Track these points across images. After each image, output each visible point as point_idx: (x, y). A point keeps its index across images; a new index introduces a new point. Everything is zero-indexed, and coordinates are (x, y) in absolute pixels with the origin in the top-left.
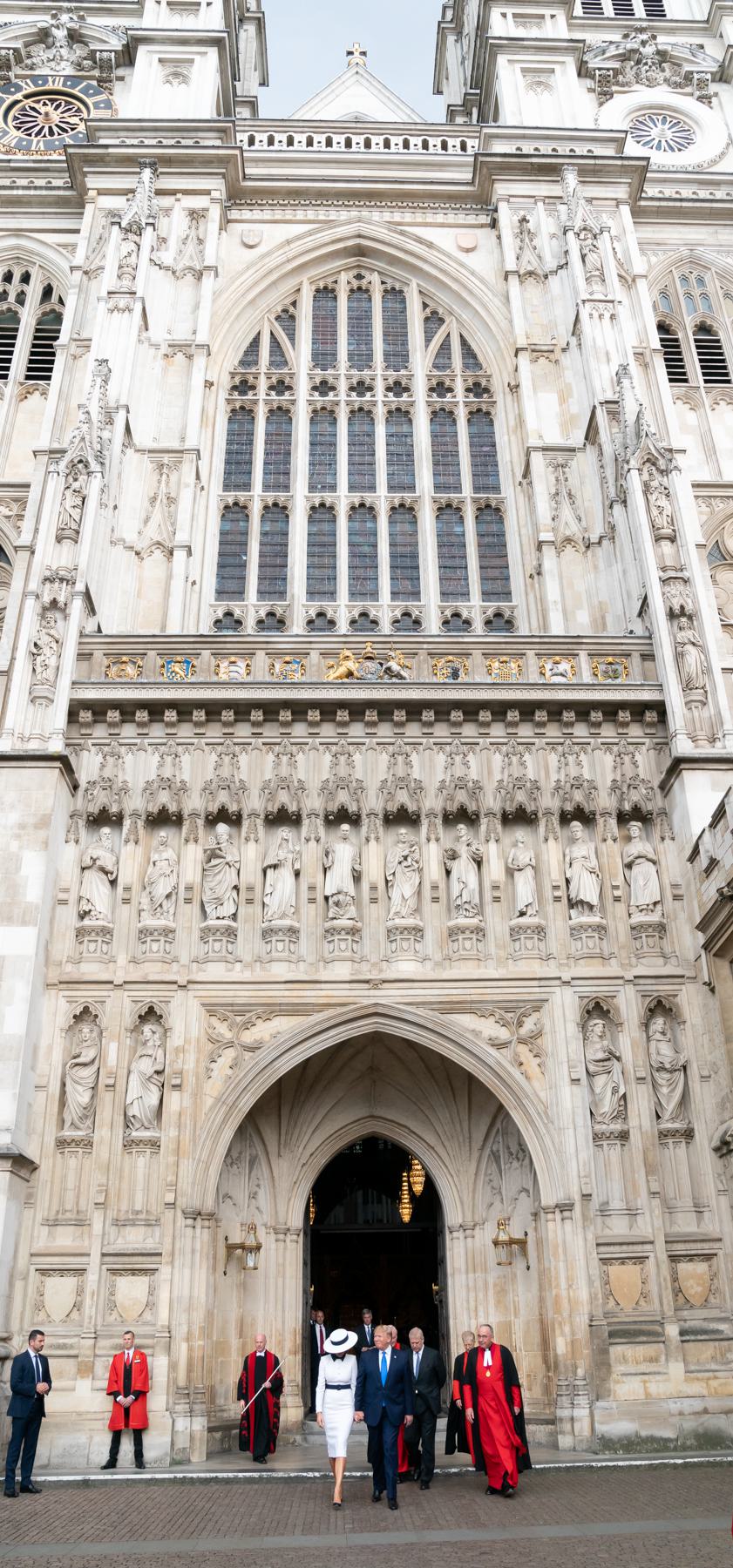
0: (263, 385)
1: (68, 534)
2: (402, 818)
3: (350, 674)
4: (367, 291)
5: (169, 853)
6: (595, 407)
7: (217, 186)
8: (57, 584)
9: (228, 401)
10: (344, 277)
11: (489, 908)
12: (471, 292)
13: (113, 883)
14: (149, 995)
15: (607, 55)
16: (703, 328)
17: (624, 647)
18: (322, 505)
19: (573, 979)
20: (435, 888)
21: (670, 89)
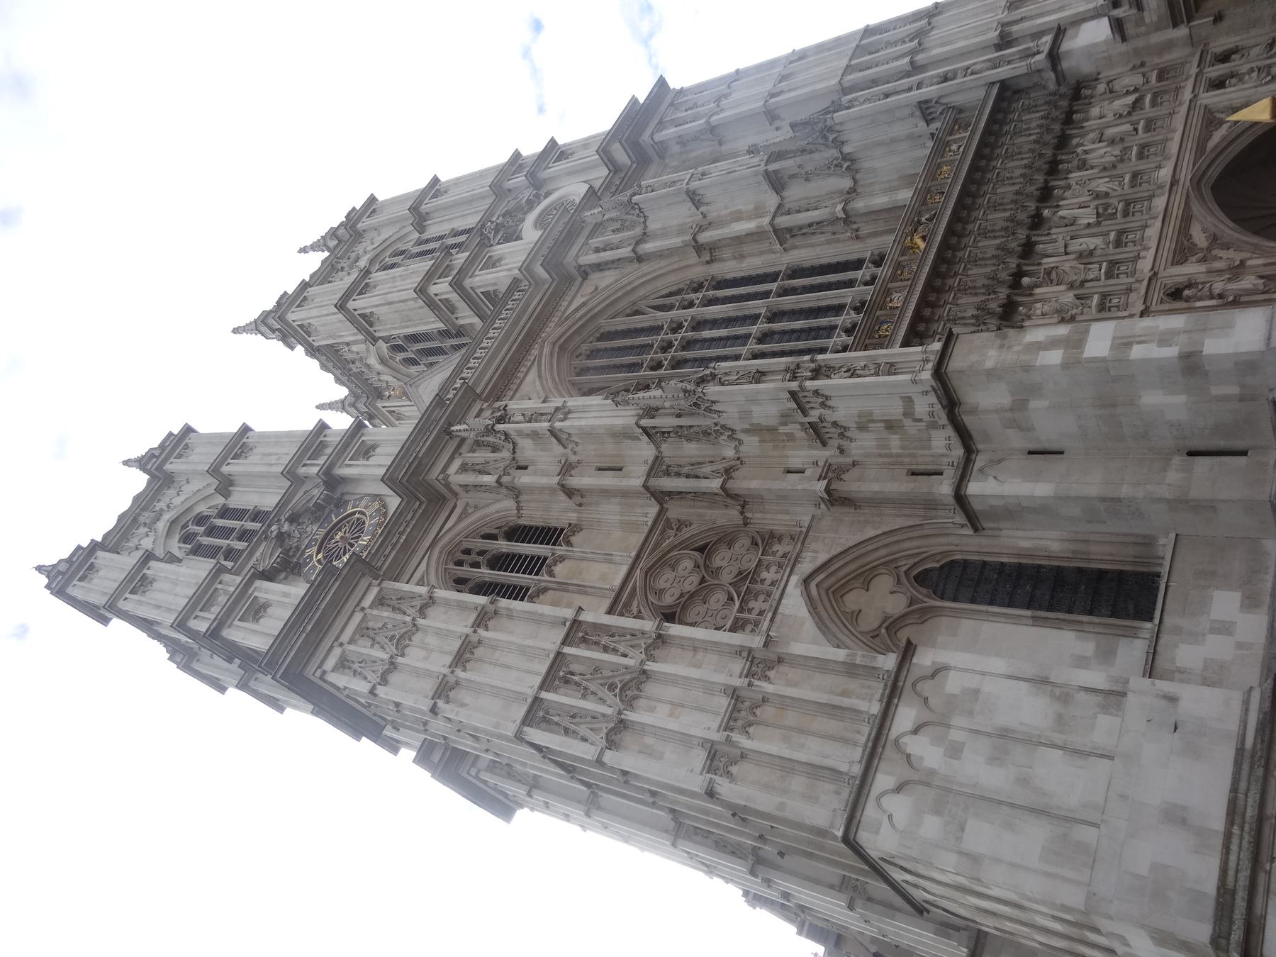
1: (759, 376)
3: (924, 238)
5: (1039, 305)
6: (766, 171)
10: (576, 362)
11: (1126, 145)
12: (629, 283)
14: (1156, 295)
17: (950, 122)
19: (1193, 91)
20: (1105, 169)
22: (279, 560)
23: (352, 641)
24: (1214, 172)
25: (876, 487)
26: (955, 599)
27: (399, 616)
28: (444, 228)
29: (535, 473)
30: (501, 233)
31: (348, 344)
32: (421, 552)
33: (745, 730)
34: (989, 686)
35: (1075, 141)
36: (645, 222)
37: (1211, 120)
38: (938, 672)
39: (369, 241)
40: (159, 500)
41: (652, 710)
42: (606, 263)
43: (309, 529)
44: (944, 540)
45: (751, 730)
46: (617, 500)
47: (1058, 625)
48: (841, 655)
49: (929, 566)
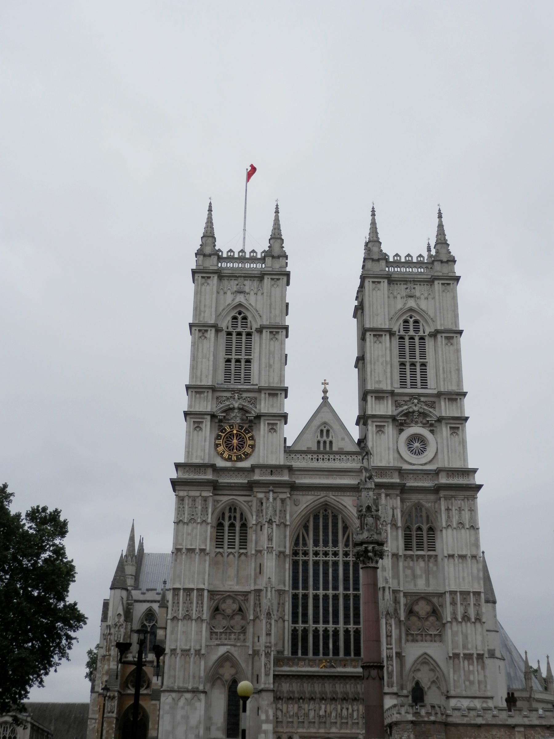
0: (301, 552)
1: (268, 634)
2: (333, 699)
3: (324, 666)
4: (328, 516)
5: (292, 706)
7: (287, 490)
8: (268, 648)
9: (292, 559)
13: (282, 712)
14: (289, 734)
15: (403, 413)
16: (419, 529)
18: (316, 594)
20: (339, 714)
21: (421, 425)
22: (221, 417)
23: (189, 497)
26: (229, 691)
27: (199, 514)
30: (405, 418)
32: (230, 492)
33: (182, 655)
35: (355, 703)
38: (200, 700)
39: (426, 295)
41: (184, 625)
43: (238, 418)
45: (183, 656)
47: (224, 717)
48: (202, 674)
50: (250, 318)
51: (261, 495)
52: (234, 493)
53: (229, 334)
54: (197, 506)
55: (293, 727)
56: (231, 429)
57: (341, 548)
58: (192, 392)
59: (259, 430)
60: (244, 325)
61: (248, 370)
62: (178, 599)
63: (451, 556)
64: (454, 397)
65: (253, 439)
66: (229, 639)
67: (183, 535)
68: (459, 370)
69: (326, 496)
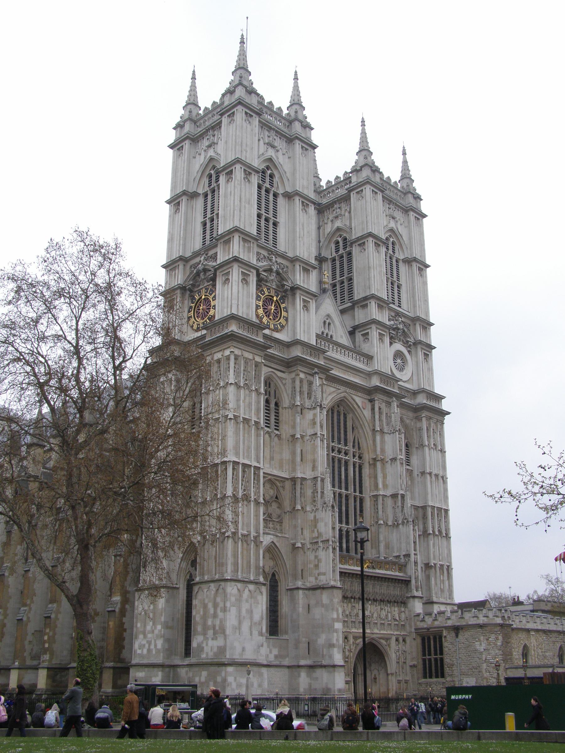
1: (333, 528)
3: (368, 566)
6: (398, 494)
10: (336, 406)
12: (365, 427)
23: (244, 358)
24: (374, 642)
25: (300, 563)
28: (403, 281)
29: (300, 420)
31: (350, 212)
34: (260, 606)
35: (389, 605)
36: (388, 433)
37: (387, 639)
40: (280, 138)
42: (374, 413)
44: (284, 580)
46: (290, 458)
48: (261, 565)
49: (277, 576)
50: (276, 179)
51: (302, 376)
52: (272, 366)
53: (259, 187)
54: (249, 370)
55: (348, 627)
56: (269, 293)
57: (350, 448)
58: (239, 237)
59: (294, 304)
60: (271, 184)
61: (275, 233)
62: (237, 475)
63: (430, 474)
64: (425, 325)
65: (287, 311)
66: (269, 528)
67: (238, 400)
68: (426, 301)
69: (346, 392)
